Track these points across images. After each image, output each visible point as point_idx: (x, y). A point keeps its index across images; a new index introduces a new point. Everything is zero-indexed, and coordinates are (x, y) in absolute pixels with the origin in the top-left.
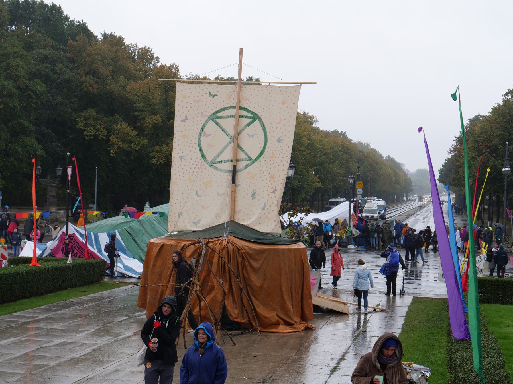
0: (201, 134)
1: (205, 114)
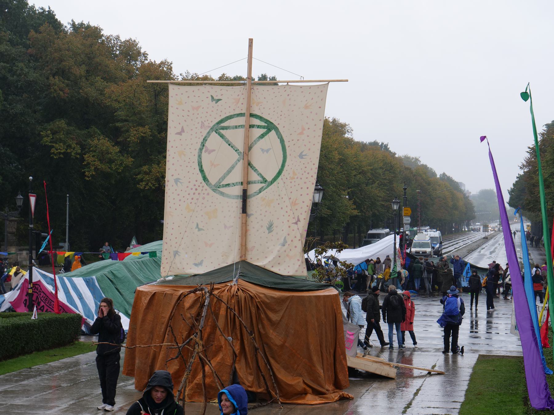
0: (201, 150)
1: (206, 124)
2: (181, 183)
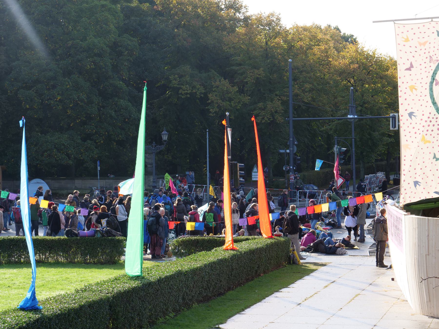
0: (432, 83)
1: (434, 58)
2: (415, 116)
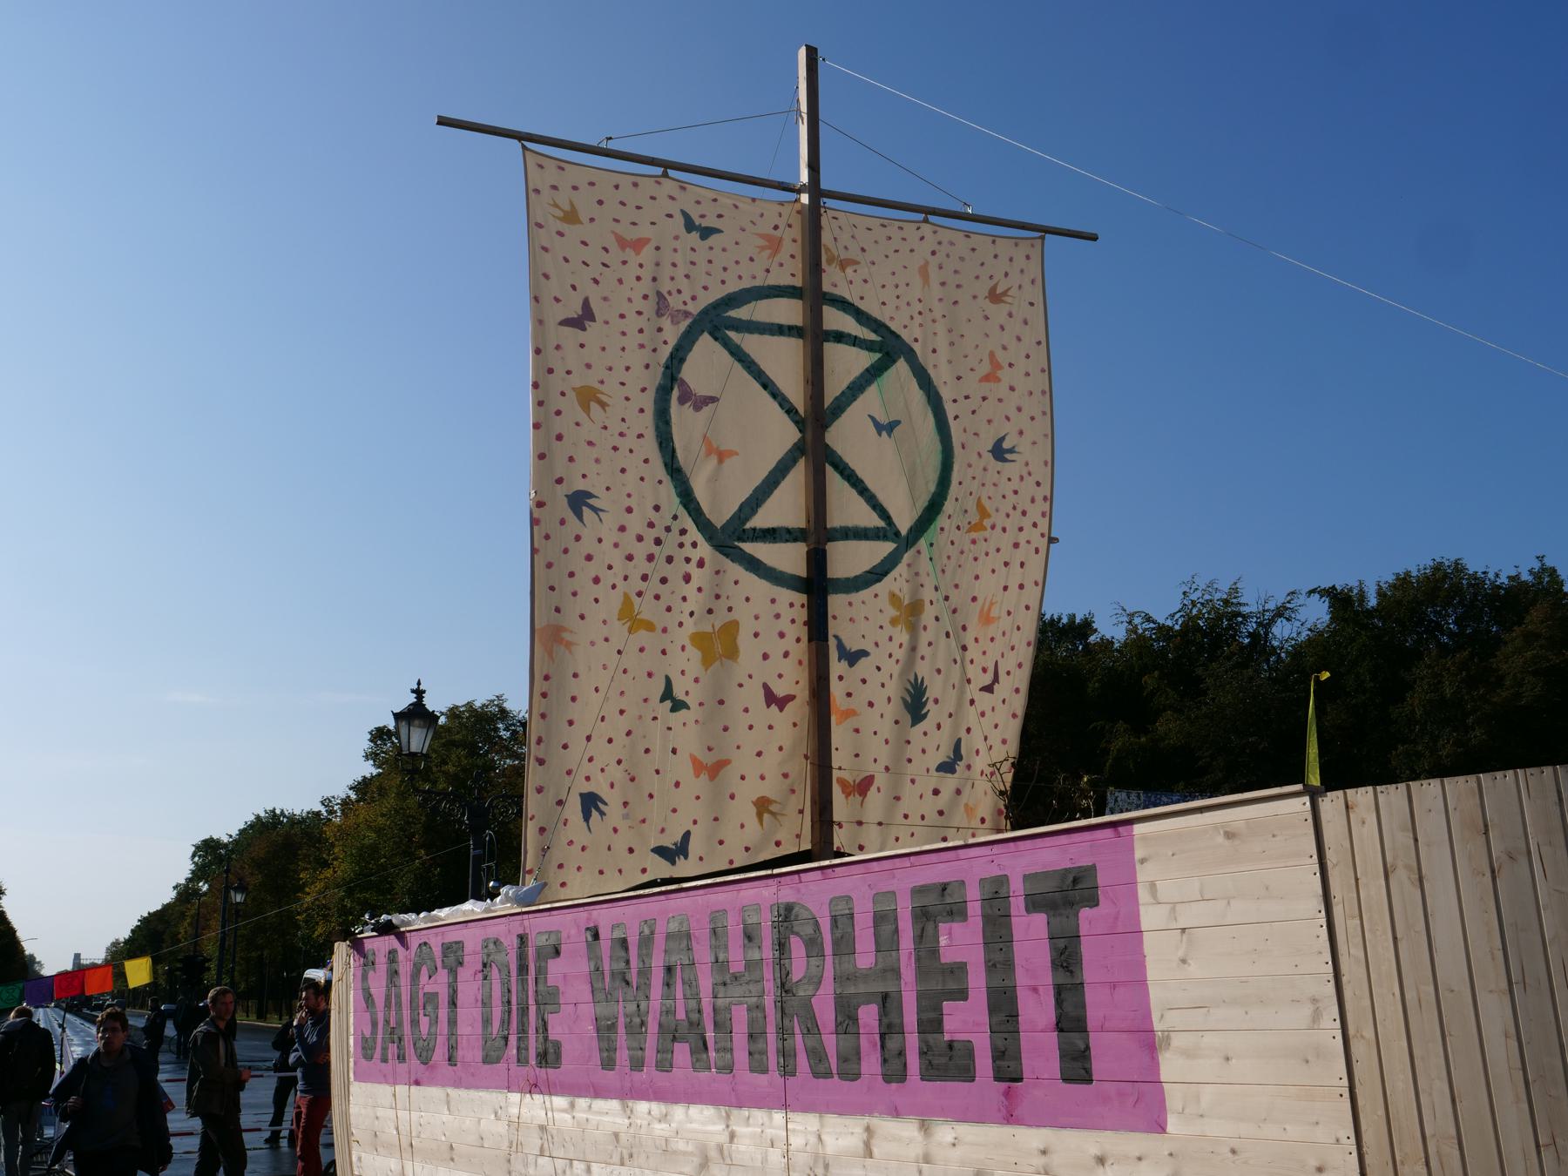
0: (663, 393)
1: (675, 302)
2: (596, 510)
